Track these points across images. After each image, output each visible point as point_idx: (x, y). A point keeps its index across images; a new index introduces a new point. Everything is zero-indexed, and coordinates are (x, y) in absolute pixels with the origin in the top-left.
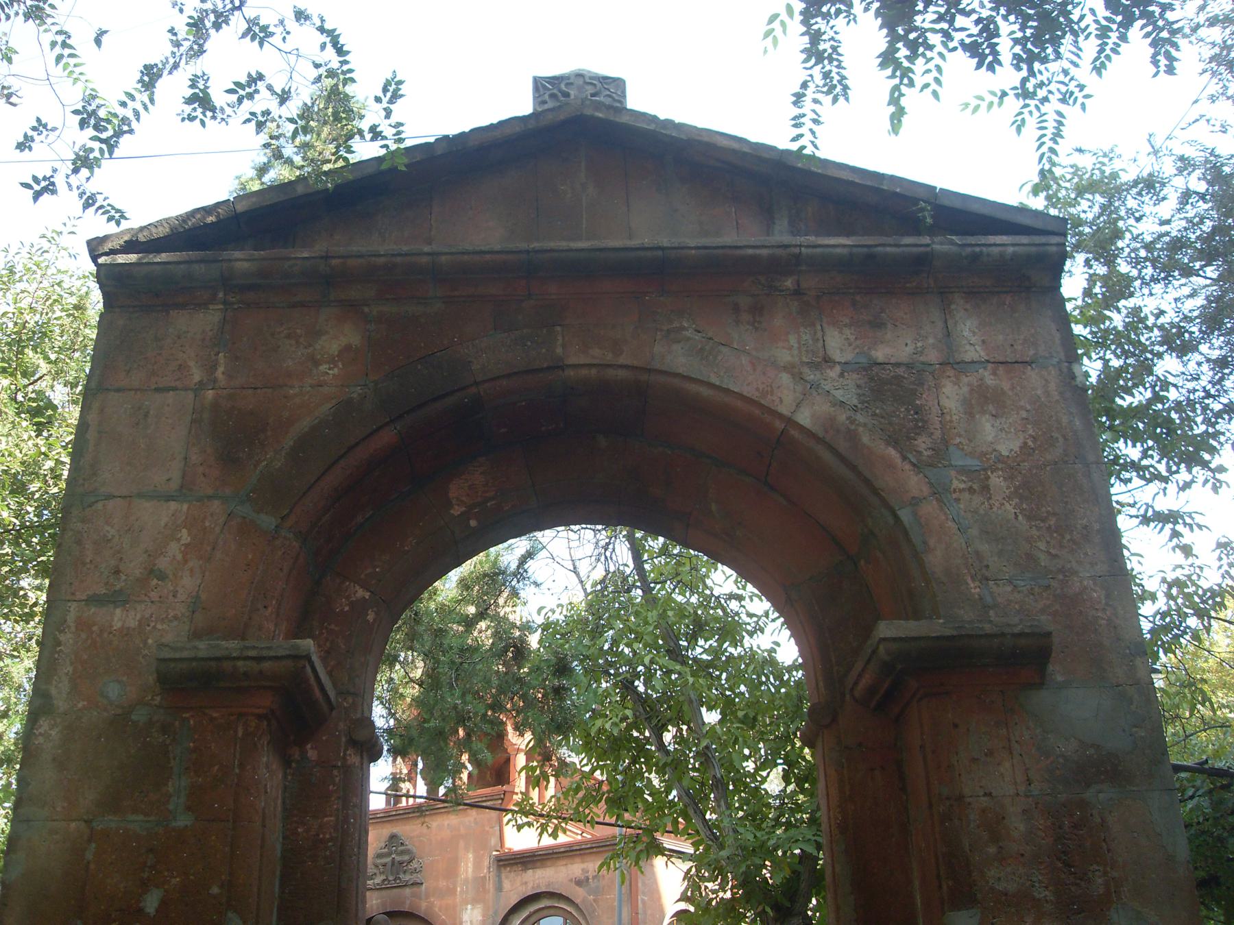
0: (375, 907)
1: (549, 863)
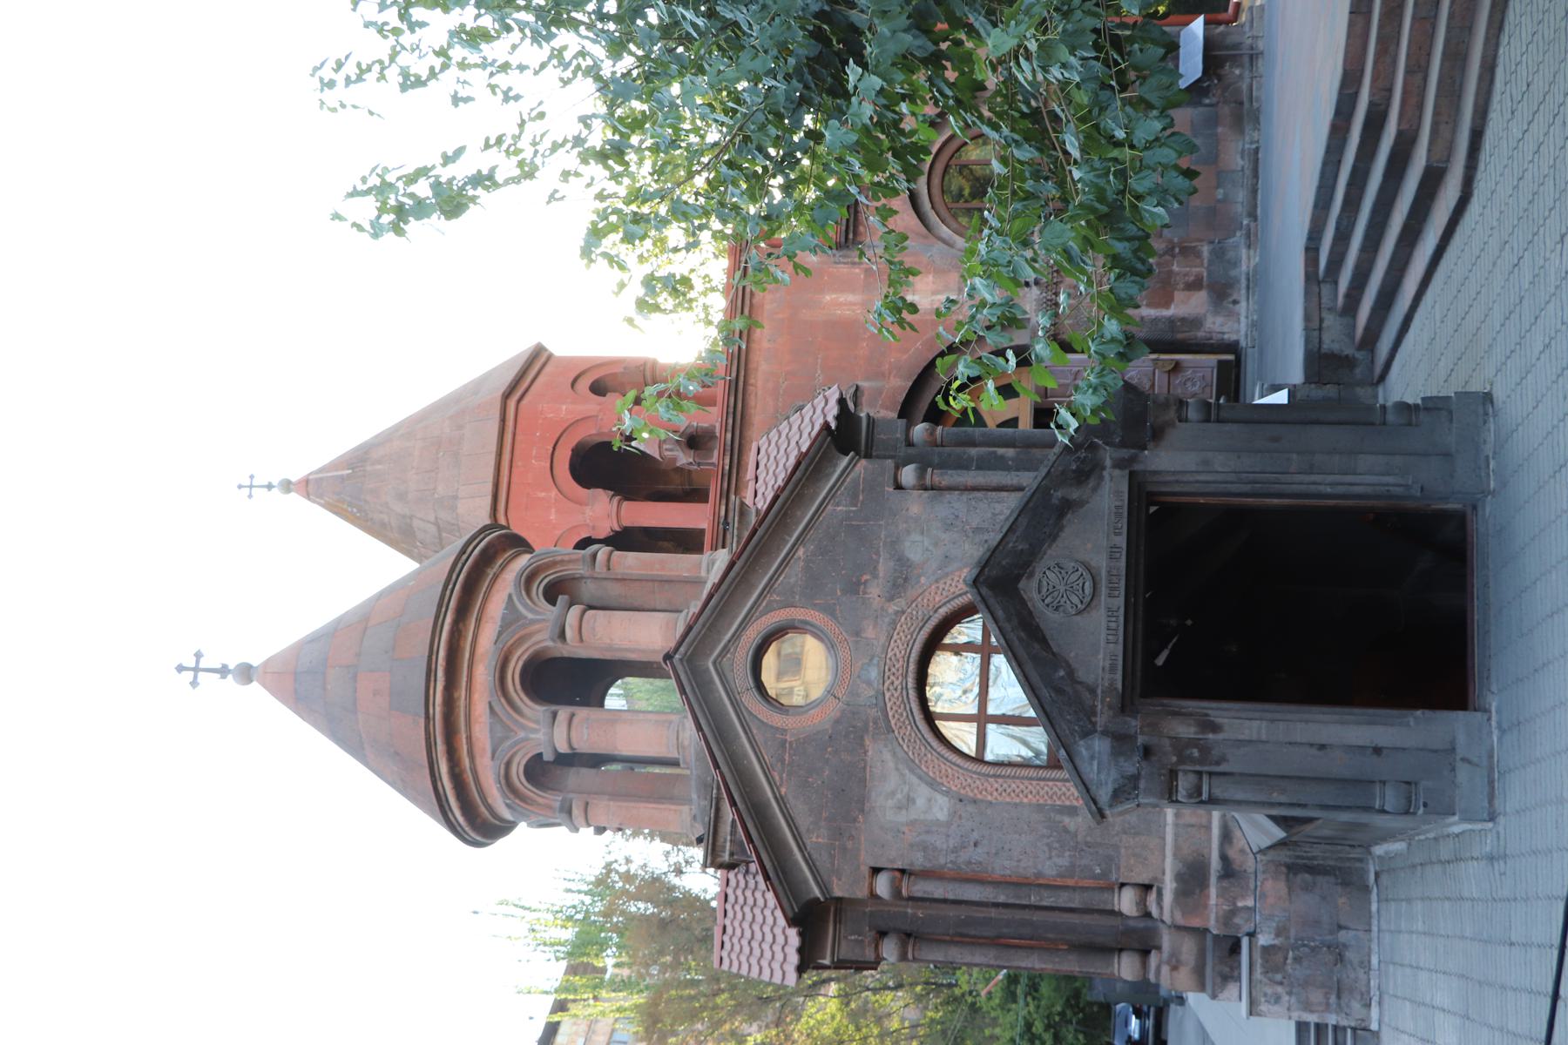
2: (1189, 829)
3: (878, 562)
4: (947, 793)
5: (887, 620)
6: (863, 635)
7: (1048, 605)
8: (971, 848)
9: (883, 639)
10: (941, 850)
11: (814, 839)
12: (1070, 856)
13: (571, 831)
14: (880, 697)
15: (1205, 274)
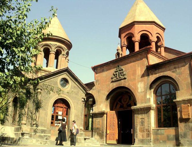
0: (114, 86)
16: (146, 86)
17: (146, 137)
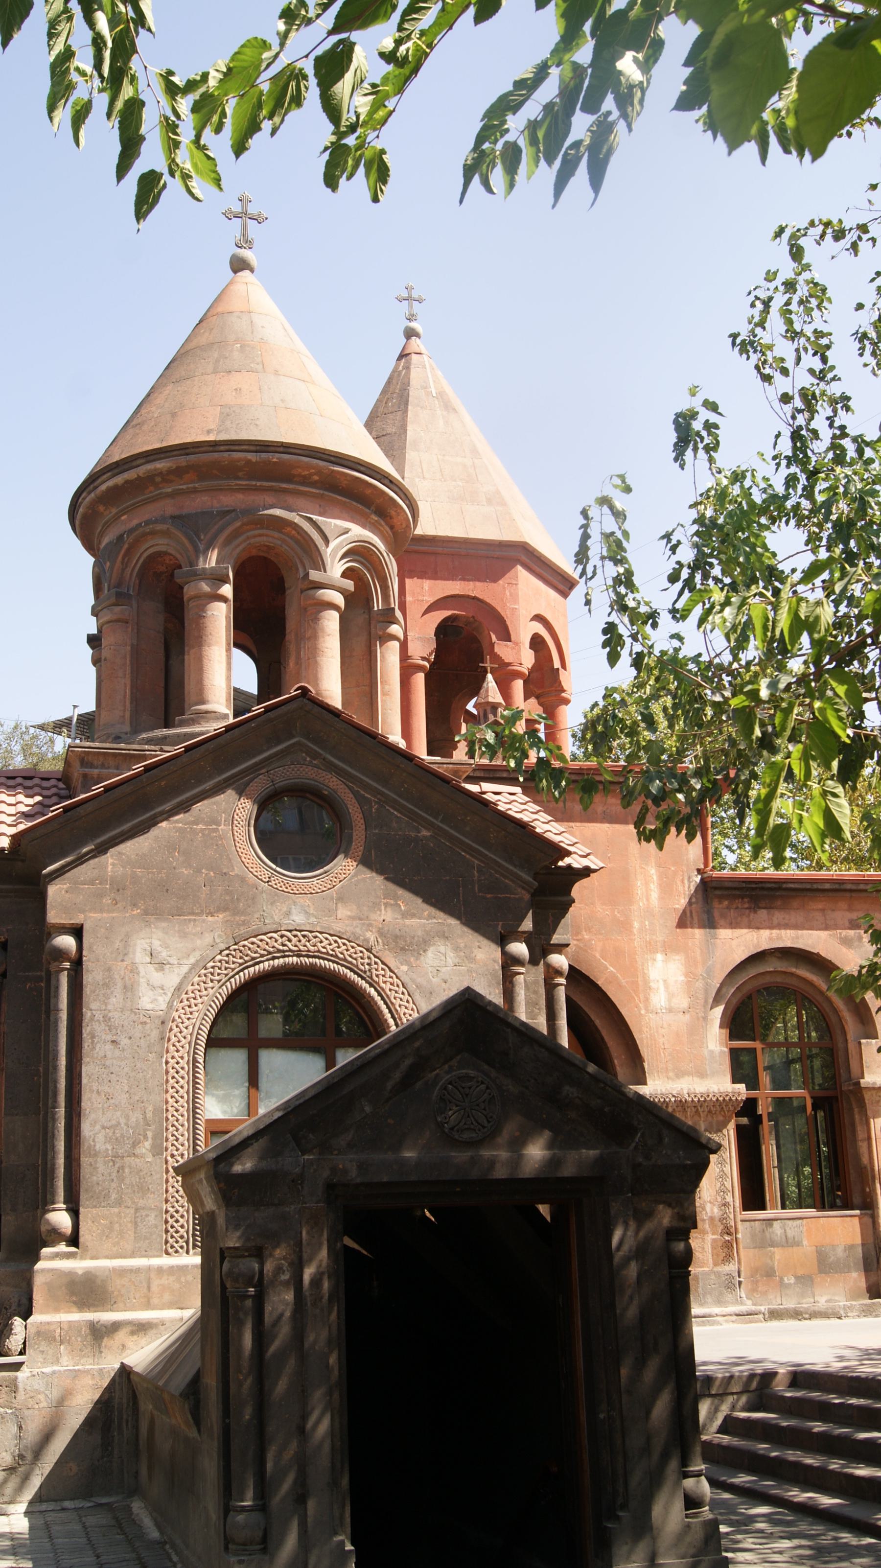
1: (795, 903)
2: (145, 1284)
3: (420, 918)
4: (170, 1006)
5: (358, 930)
6: (339, 905)
7: (445, 1089)
8: (109, 1037)
9: (337, 927)
10: (106, 1004)
11: (110, 861)
12: (107, 1150)
13: (93, 608)
14: (274, 927)
15: (706, 1269)
16: (700, 984)
17: (712, 1265)
